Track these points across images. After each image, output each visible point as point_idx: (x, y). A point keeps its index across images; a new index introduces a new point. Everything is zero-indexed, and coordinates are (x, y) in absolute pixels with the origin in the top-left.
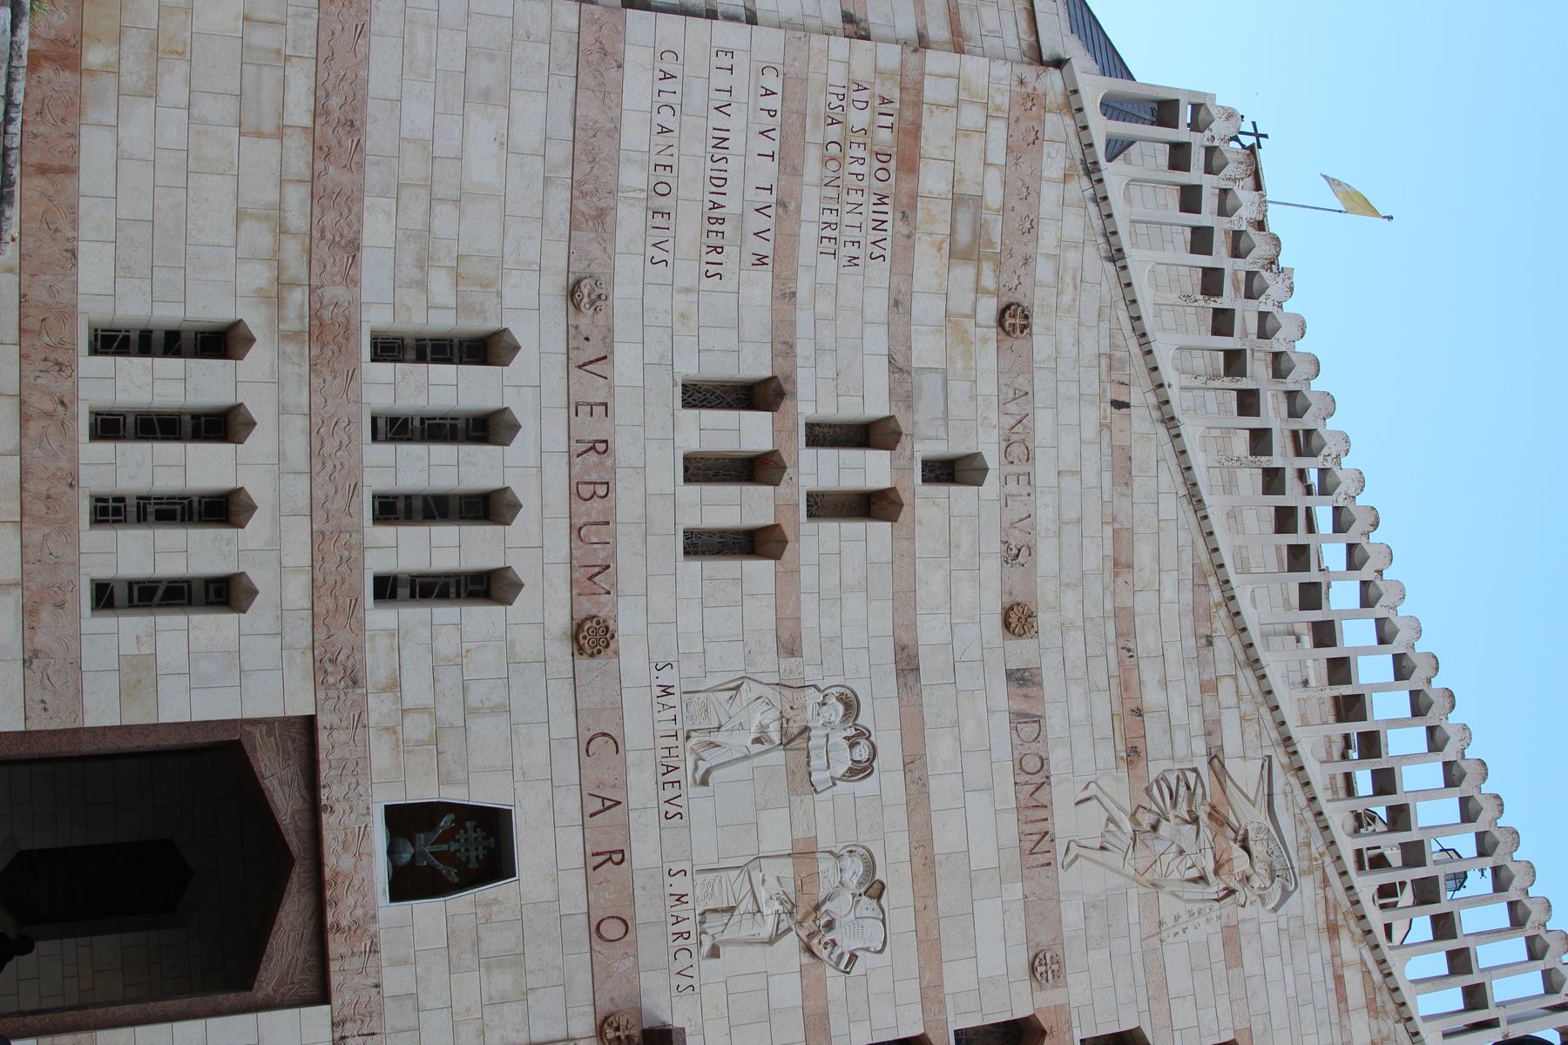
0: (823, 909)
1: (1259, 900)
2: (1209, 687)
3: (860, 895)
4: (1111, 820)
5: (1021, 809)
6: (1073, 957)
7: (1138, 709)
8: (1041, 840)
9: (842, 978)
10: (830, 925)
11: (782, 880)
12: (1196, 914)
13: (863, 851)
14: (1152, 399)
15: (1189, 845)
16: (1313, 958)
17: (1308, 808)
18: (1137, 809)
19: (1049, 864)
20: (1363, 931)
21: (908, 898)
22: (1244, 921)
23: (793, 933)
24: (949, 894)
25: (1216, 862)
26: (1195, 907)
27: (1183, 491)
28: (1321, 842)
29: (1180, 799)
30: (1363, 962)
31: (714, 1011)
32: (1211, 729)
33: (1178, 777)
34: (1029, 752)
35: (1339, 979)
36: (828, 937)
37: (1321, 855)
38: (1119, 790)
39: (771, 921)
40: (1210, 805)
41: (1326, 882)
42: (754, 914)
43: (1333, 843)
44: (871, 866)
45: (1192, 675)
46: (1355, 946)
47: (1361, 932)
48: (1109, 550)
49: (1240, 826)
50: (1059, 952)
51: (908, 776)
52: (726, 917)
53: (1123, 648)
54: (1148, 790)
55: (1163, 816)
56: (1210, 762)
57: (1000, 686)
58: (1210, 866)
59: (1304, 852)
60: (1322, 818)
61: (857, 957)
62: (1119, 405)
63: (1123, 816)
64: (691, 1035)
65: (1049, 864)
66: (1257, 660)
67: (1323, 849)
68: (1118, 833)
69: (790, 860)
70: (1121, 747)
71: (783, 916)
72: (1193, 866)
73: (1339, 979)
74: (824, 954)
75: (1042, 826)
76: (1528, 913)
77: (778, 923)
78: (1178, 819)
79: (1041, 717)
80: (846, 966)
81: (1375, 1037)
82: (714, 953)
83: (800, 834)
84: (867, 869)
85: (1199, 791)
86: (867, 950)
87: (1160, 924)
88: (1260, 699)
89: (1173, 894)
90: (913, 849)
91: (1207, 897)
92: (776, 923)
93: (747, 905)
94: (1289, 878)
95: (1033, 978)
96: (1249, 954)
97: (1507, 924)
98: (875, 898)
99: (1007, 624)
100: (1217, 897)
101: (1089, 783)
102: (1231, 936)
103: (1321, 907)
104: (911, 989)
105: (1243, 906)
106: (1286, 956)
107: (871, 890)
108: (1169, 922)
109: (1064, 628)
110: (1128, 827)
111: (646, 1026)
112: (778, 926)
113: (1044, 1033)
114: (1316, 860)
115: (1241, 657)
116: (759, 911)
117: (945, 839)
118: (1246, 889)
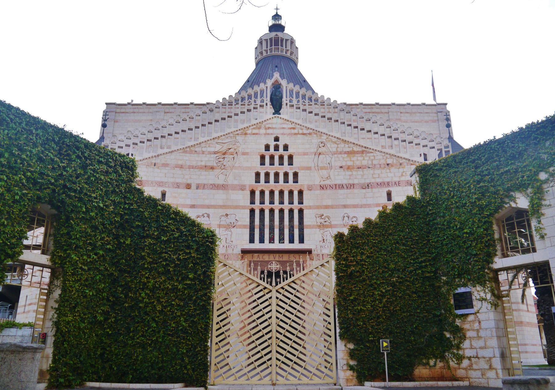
2: (203, 153)
10: (231, 223)
14: (154, 158)
16: (250, 138)
21: (228, 210)
24: (229, 203)
27: (170, 154)
30: (252, 129)
32: (210, 153)
35: (254, 134)
36: (232, 223)
38: (217, 171)
44: (222, 216)
45: (201, 155)
48: (178, 169)
54: (218, 166)
55: (222, 164)
57: (199, 191)
58: (232, 156)
62: (155, 165)
73: (254, 134)
74: (235, 224)
82: (232, 241)
93: (226, 236)
96: (247, 151)
99: (189, 189)
102: (244, 154)
103: (242, 136)
104: (243, 211)
109: (191, 178)
110: (223, 171)
115: (199, 146)
117: (221, 203)
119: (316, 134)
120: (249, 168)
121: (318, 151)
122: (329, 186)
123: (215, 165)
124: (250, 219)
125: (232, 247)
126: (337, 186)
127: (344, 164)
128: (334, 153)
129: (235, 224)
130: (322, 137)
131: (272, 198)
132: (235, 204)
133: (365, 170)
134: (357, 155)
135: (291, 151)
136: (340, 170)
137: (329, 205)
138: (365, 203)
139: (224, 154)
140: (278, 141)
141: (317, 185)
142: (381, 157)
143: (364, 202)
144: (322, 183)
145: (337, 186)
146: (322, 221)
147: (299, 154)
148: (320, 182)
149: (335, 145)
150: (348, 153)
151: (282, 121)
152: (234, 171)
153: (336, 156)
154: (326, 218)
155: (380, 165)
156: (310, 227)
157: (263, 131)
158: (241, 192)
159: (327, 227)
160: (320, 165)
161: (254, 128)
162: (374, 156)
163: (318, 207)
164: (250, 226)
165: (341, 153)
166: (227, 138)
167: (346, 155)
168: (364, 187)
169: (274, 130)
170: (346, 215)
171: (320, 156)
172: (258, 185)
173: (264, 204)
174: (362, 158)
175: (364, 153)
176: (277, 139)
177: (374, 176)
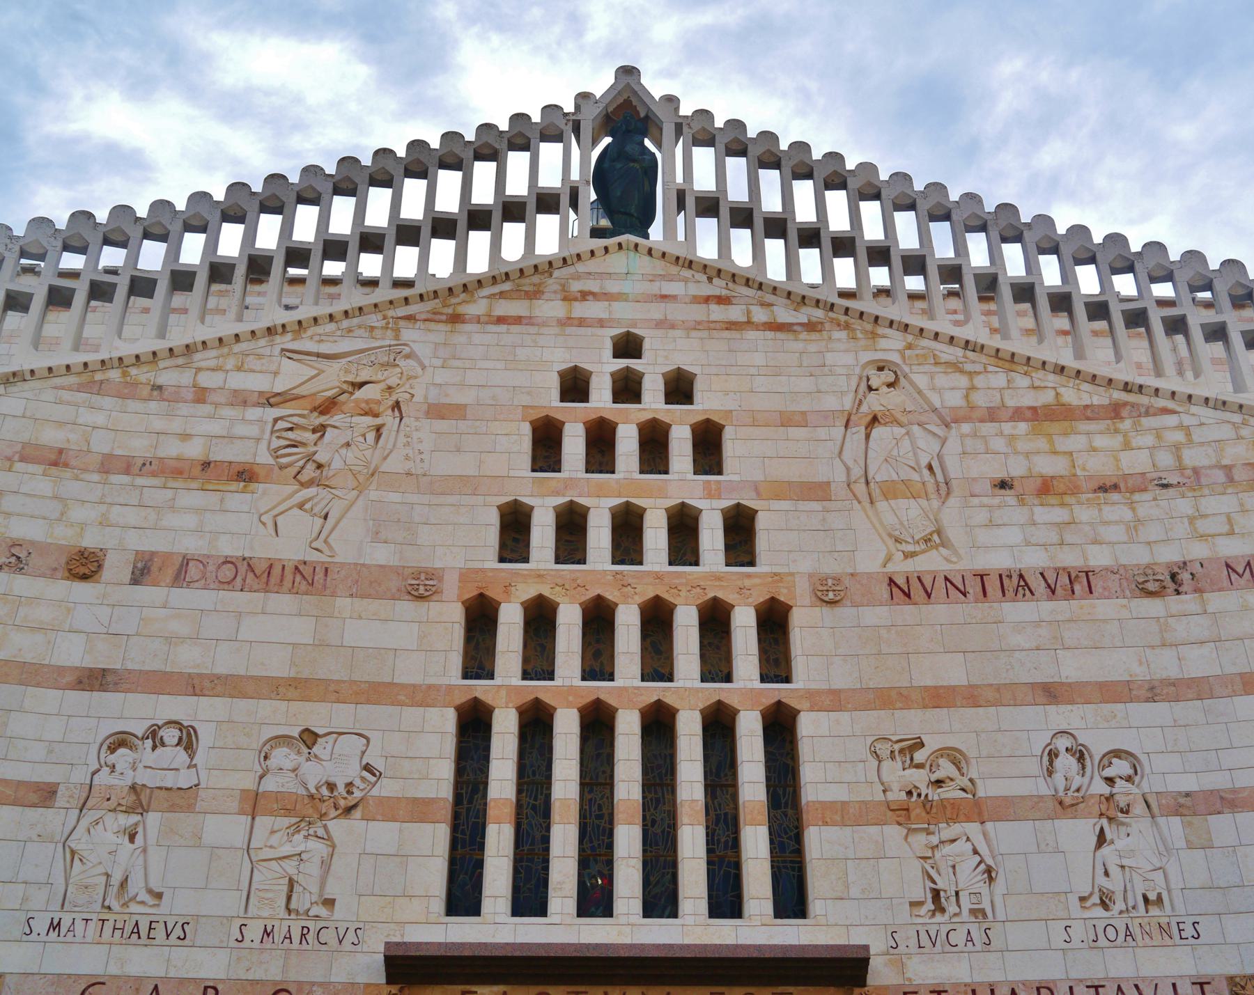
0: (313, 791)
1: (411, 381)
2: (201, 395)
3: (310, 753)
4: (301, 506)
5: (268, 589)
6: (416, 559)
7: (203, 465)
8: (301, 574)
9: (384, 781)
10: (331, 787)
11: (276, 828)
12: (409, 440)
13: (268, 746)
15: (346, 436)
17: (339, 323)
18: (298, 481)
19: (326, 570)
20: (464, 291)
22: (426, 397)
23: (330, 824)
24: (331, 669)
25: (366, 414)
26: (402, 440)
28: (373, 316)
29: (299, 439)
30: (489, 297)
31: (385, 910)
32: (241, 399)
33: (278, 437)
34: (214, 574)
35: (501, 320)
36: (341, 789)
37: (385, 318)
39: (313, 844)
40: (312, 412)
41: (410, 318)
42: (302, 860)
43: (376, 306)
46: (475, 301)
47: (464, 294)
49: (338, 387)
50: (410, 571)
51: (207, 693)
52: (297, 888)
53: (140, 470)
54: (281, 468)
55: (309, 458)
56: (272, 406)
58: (368, 420)
59: (377, 333)
60: (350, 312)
61: (368, 764)
63: (302, 492)
64: (402, 936)
65: (326, 570)
66: (187, 346)
67: (380, 316)
68: (315, 500)
69: (257, 819)
70: (234, 486)
71: (311, 832)
72: (364, 436)
73: (501, 320)
74: (358, 794)
75: (288, 571)
76: (487, 145)
77: (317, 836)
78: (319, 443)
79: (184, 557)
80: (374, 775)
81: (559, 296)
82: (330, 903)
83: (234, 805)
84: (286, 744)
85: (295, 419)
86: (363, 753)
87: (409, 474)
88: (226, 350)
89: (385, 458)
90: (279, 697)
91: (395, 428)
92: (316, 839)
94: (398, 351)
95: (429, 599)
96: (457, 398)
97: (494, 164)
98: (316, 740)
100: (398, 419)
101: (261, 521)
102: (437, 411)
103: (433, 325)
104: (412, 715)
105: (413, 396)
106: (467, 364)
107: (308, 743)
108: (409, 465)
110: (311, 491)
111: (383, 981)
112: (320, 838)
113: (481, 595)
114: (388, 323)
116: (300, 855)
117: (277, 666)
118: (397, 391)
119: (847, 326)
120: (468, 484)
121: (864, 408)
122: (940, 582)
123: (264, 458)
124: (460, 771)
125: (329, 936)
126: (993, 586)
127: (1016, 468)
128: (949, 420)
129: (358, 794)
130: (883, 343)
131: (597, 655)
132: (369, 672)
133: (1147, 496)
134: (1083, 426)
135: (706, 403)
136: (996, 501)
137: (953, 689)
138: (1173, 673)
139: (327, 407)
140: (638, 355)
141: (869, 575)
142: (1226, 432)
143: (1166, 665)
144: (900, 568)
145: (993, 586)
146: (919, 778)
147: (756, 419)
148: (889, 559)
149: (957, 374)
150: (1035, 415)
151: (659, 266)
152: (373, 494)
153: (966, 428)
154: (944, 762)
155: (1228, 469)
156: (840, 814)
157: (549, 308)
158: (407, 608)
159: (951, 812)
160: (880, 473)
161: (502, 295)
162: (1187, 430)
163: (886, 699)
164: (456, 816)
165: (992, 415)
166: (350, 330)
167: (1023, 427)
168: (1151, 586)
169: (616, 305)
170: (1062, 743)
171: (877, 432)
172: (516, 573)
173: (550, 676)
174: (1115, 442)
175: (1124, 413)
176: (628, 346)
177: (1203, 526)
